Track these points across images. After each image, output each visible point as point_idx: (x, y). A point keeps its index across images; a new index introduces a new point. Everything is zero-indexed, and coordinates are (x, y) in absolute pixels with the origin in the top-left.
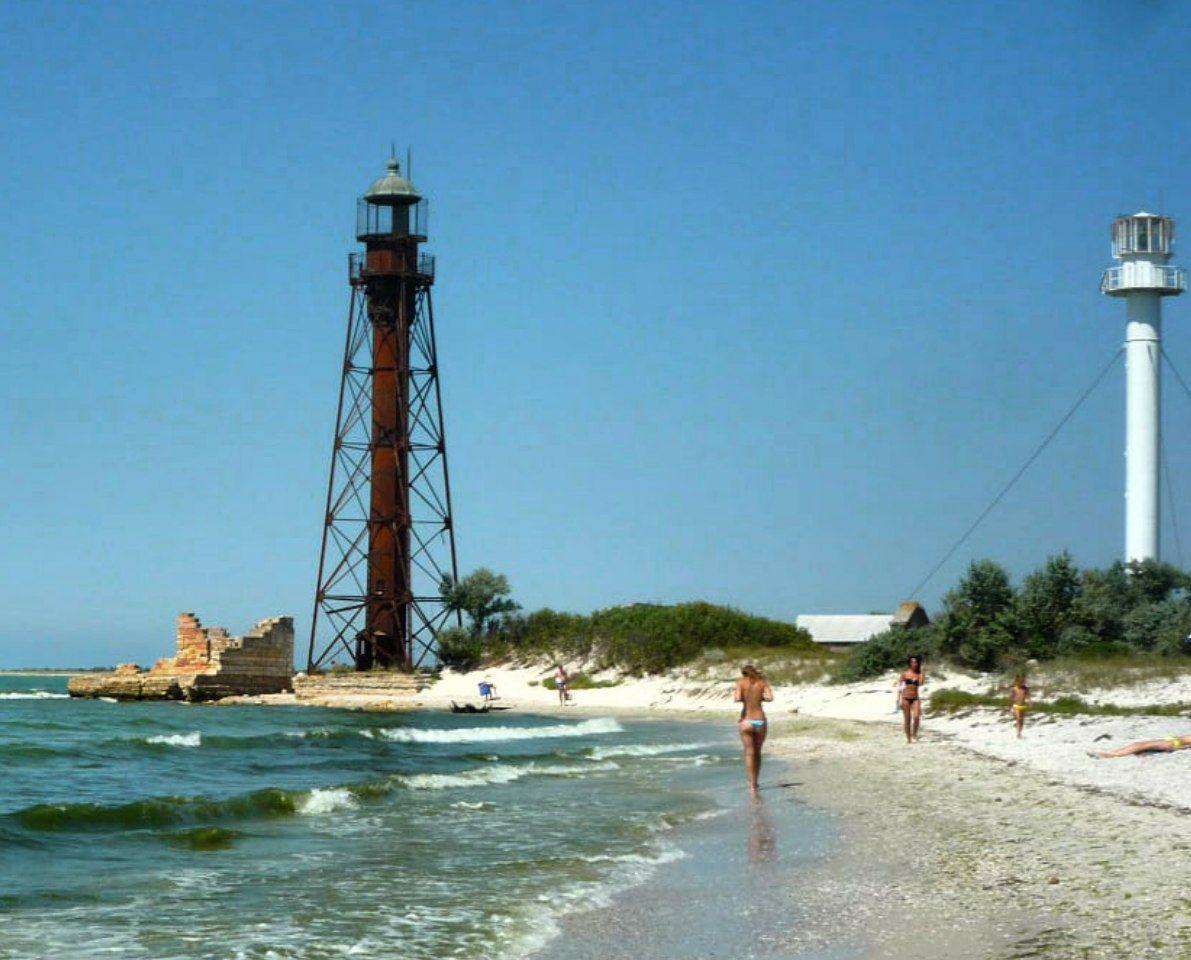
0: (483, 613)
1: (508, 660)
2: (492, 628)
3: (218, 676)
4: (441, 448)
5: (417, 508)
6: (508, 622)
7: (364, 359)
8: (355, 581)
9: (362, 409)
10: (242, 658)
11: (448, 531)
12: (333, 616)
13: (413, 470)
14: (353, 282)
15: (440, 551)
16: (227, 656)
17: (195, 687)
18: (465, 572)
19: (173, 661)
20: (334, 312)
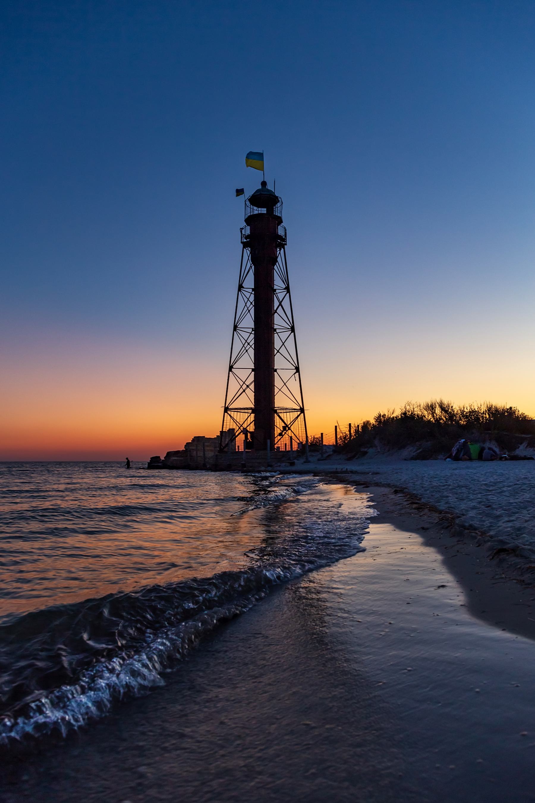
4: (293, 329)
5: (279, 362)
7: (250, 282)
8: (247, 400)
13: (277, 344)
14: (245, 245)
15: (294, 385)
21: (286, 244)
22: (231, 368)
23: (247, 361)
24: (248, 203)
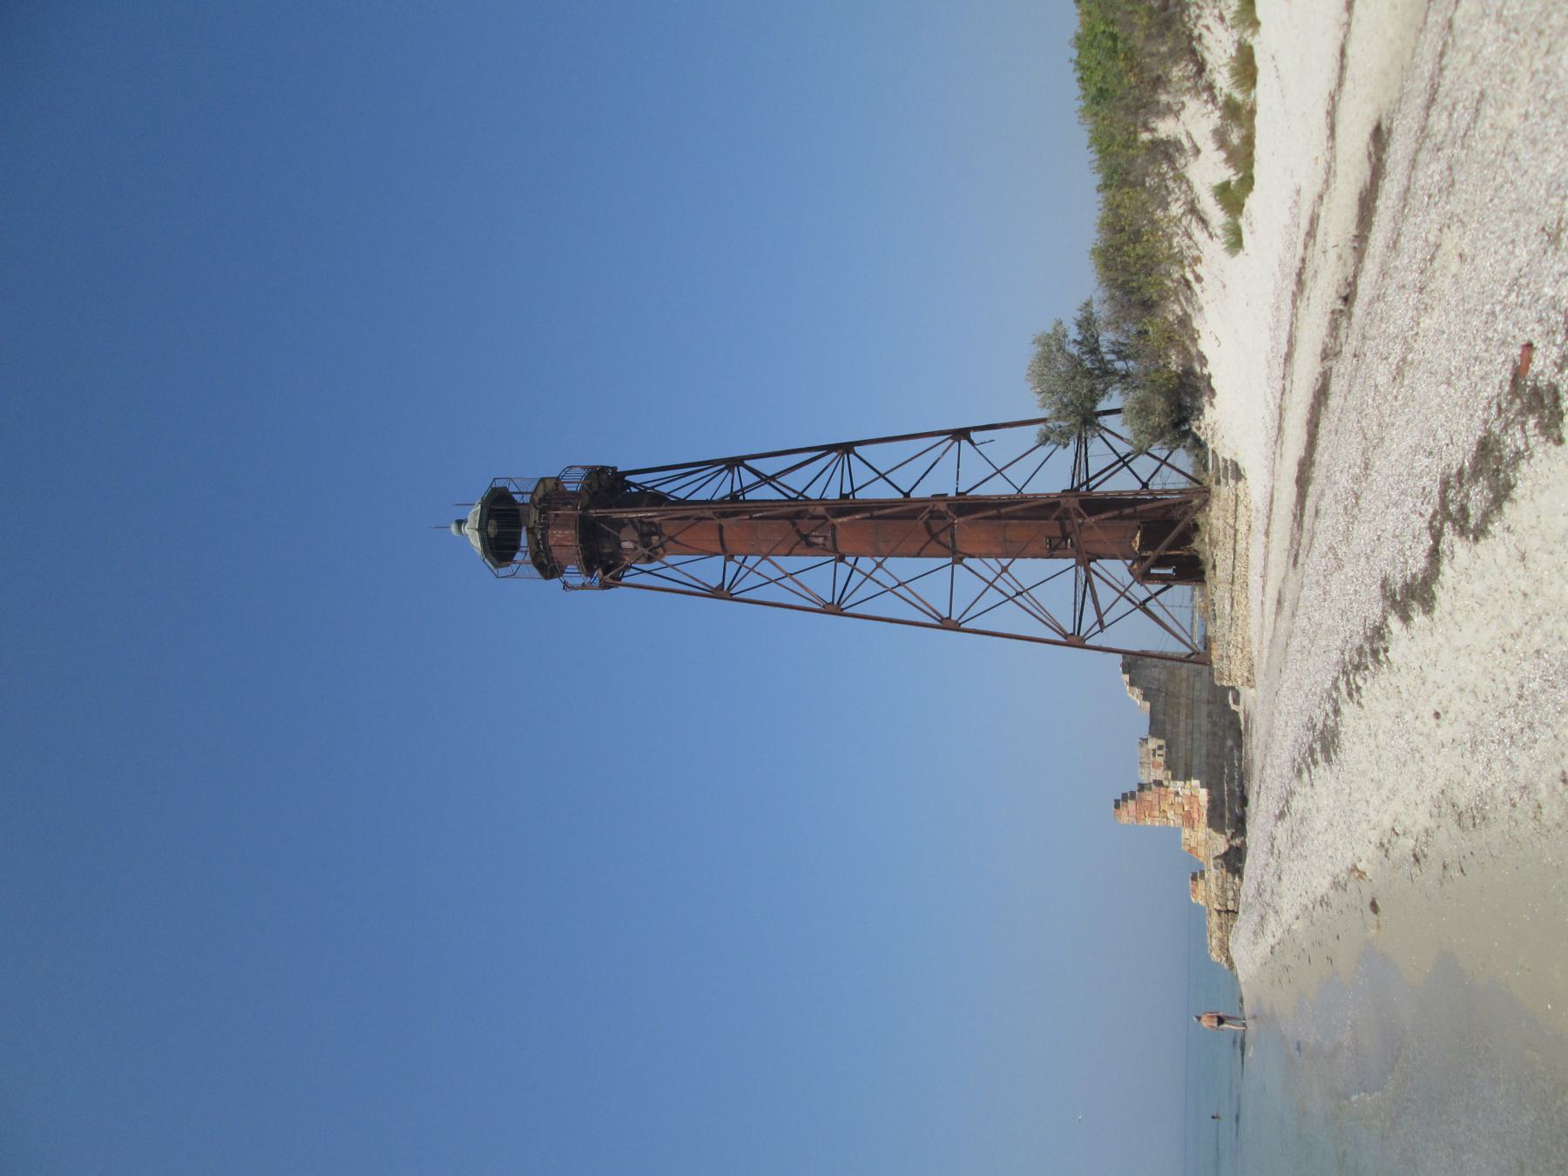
0: (1106, 372)
1: (1184, 321)
2: (1135, 362)
3: (1207, 785)
4: (846, 448)
6: (1114, 324)
7: (710, 570)
8: (1050, 580)
9: (776, 574)
10: (1182, 738)
11: (974, 435)
12: (1107, 620)
15: (1003, 446)
16: (1180, 768)
17: (1229, 833)
18: (1031, 404)
19: (1186, 833)
20: (649, 619)
22: (948, 624)
23: (931, 579)
24: (503, 571)
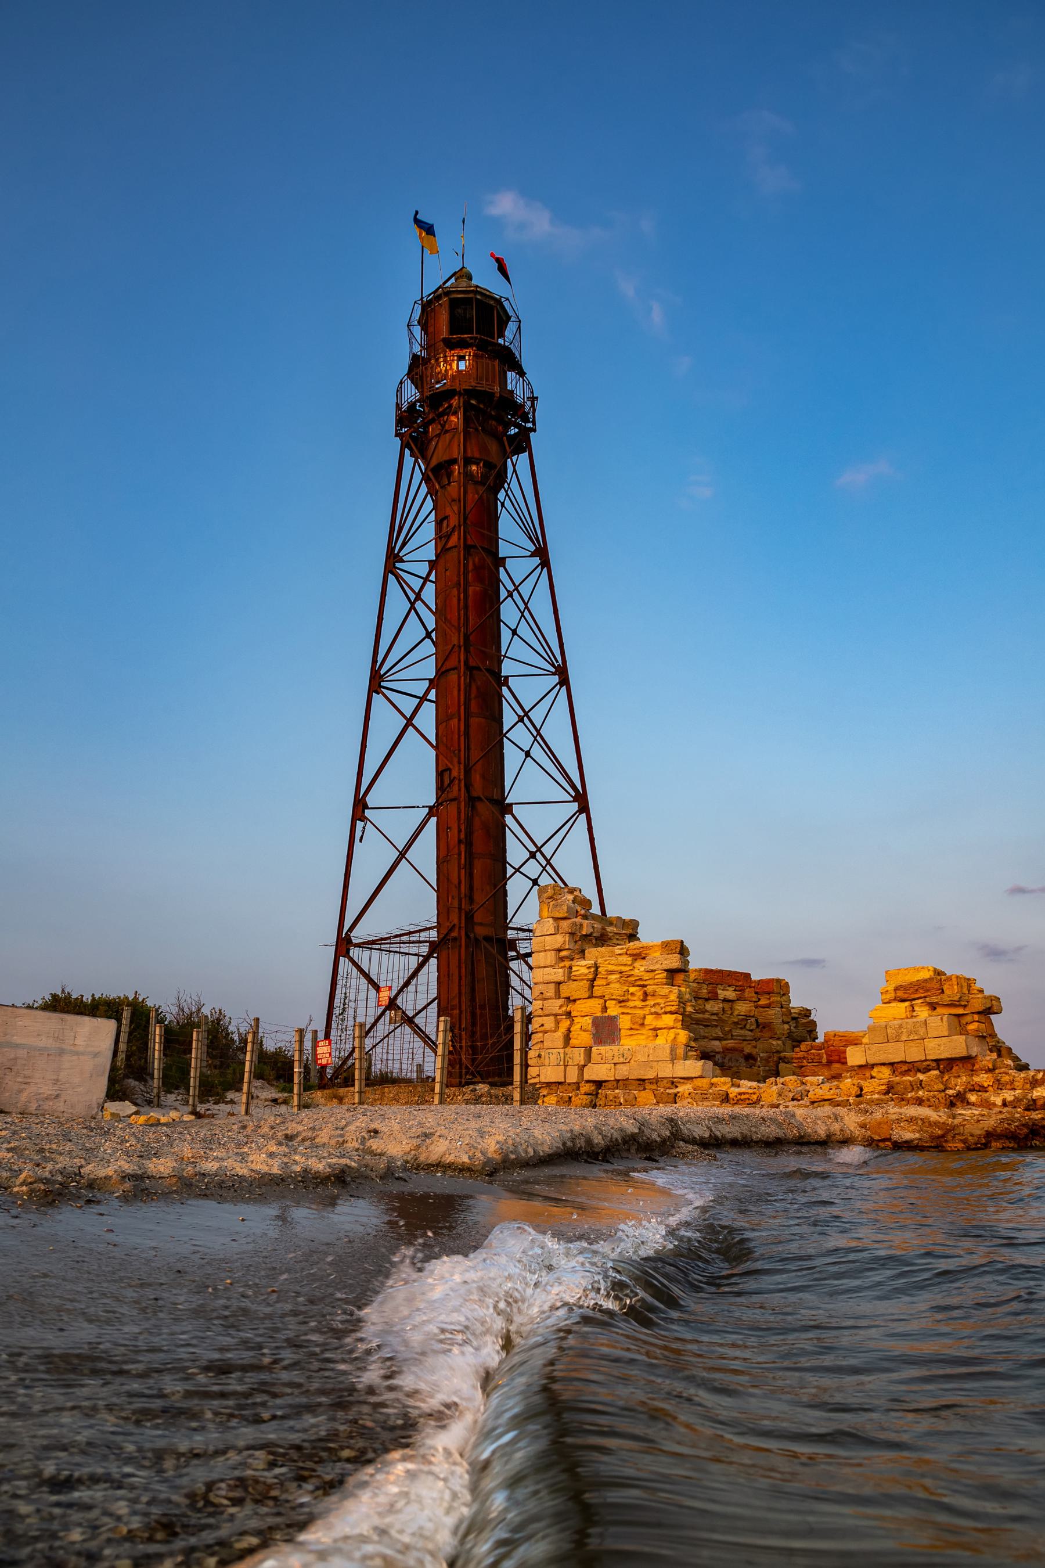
7: (422, 547)
21: (535, 431)
